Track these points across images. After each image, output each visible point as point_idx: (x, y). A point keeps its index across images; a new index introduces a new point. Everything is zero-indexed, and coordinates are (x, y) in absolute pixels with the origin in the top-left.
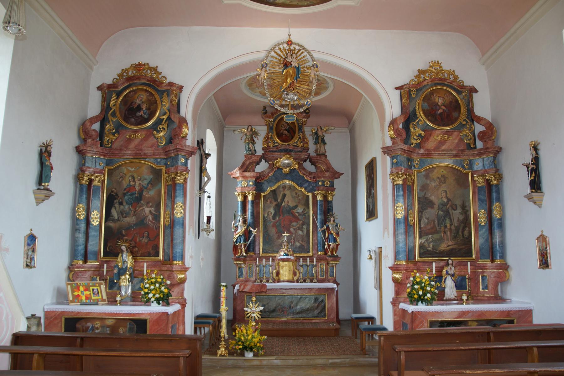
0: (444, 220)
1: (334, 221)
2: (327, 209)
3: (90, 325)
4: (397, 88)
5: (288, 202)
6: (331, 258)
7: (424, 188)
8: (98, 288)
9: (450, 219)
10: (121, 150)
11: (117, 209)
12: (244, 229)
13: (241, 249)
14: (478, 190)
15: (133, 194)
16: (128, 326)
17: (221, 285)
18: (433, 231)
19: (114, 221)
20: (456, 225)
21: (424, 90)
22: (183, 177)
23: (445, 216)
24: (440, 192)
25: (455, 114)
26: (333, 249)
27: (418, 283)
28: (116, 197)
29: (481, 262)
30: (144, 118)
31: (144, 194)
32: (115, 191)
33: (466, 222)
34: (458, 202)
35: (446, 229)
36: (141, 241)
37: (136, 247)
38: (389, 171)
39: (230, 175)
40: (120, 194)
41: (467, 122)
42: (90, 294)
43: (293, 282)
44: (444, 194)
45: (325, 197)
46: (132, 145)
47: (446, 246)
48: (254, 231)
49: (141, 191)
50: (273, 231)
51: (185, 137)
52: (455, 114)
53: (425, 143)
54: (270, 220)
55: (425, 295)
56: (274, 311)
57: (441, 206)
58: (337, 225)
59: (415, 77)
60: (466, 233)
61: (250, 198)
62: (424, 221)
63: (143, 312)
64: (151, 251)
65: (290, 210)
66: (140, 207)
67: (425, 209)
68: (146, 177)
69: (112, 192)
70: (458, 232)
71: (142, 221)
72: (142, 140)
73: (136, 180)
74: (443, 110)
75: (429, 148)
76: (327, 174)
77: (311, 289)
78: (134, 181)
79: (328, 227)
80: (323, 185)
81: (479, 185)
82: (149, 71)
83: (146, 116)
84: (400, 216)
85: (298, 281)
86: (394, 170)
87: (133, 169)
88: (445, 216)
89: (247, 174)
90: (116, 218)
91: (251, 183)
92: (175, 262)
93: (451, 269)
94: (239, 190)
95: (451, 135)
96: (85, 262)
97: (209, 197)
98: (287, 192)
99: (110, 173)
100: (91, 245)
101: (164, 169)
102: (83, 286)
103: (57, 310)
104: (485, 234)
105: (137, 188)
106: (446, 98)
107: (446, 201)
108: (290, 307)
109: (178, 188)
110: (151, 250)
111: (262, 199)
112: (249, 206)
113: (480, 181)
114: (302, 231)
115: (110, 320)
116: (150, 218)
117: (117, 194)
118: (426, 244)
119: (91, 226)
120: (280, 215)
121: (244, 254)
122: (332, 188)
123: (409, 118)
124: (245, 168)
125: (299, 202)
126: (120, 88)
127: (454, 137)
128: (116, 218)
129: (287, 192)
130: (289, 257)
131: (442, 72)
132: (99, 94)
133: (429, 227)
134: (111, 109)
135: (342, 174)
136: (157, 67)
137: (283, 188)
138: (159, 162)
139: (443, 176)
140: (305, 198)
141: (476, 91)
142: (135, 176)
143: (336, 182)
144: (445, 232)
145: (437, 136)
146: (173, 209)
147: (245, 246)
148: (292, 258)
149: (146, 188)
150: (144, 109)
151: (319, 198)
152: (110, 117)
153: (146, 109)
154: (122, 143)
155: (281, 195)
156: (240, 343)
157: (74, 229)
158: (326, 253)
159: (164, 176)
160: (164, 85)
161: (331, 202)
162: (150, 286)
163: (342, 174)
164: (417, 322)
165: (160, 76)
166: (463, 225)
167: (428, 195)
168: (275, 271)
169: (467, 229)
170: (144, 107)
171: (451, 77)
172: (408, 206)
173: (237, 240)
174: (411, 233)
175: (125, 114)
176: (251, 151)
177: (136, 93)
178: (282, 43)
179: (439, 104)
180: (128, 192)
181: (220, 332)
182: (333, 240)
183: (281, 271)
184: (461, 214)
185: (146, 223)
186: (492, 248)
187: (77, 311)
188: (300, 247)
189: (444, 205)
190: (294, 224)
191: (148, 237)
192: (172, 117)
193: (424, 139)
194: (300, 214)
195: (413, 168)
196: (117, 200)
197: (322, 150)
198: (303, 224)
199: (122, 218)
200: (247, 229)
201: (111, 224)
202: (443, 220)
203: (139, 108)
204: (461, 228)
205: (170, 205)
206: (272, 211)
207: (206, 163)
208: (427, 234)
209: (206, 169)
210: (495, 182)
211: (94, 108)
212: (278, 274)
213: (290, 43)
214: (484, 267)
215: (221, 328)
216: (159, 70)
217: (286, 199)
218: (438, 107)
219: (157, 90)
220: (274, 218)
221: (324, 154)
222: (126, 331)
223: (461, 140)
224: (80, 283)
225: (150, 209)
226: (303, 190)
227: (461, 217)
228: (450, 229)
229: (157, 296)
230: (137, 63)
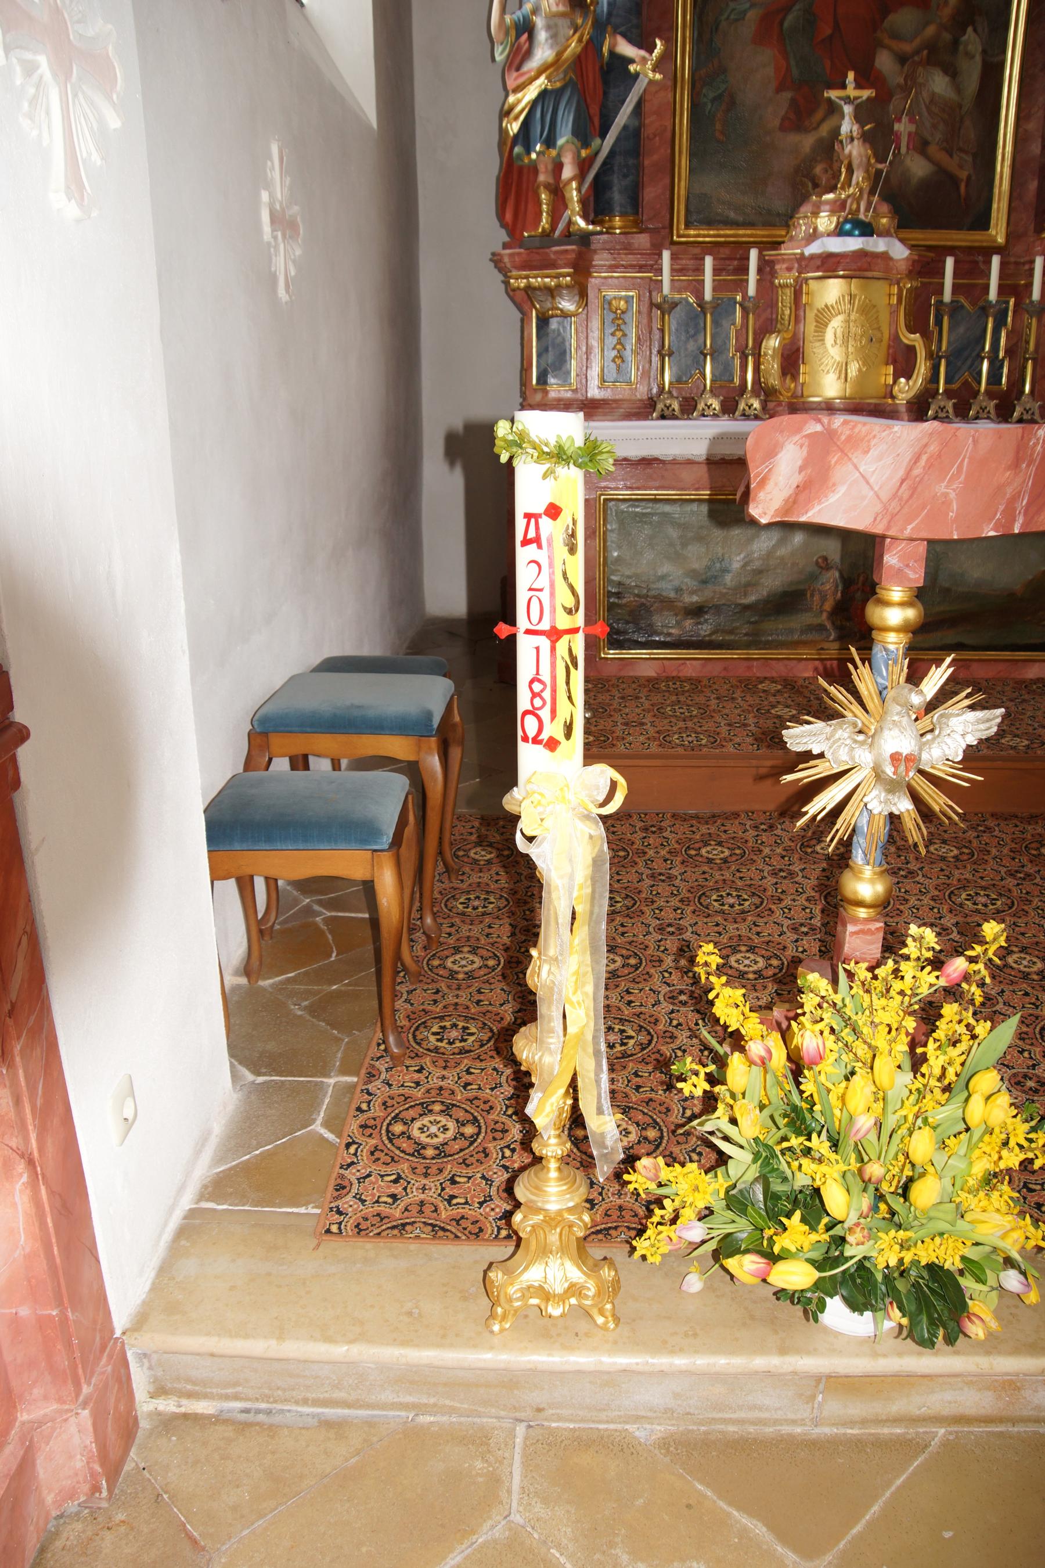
48: (644, 64)
121: (582, 223)
130: (878, 245)
148: (899, 251)
168: (773, 343)
173: (526, 125)
188: (925, 185)
200: (592, 46)
212: (792, 359)
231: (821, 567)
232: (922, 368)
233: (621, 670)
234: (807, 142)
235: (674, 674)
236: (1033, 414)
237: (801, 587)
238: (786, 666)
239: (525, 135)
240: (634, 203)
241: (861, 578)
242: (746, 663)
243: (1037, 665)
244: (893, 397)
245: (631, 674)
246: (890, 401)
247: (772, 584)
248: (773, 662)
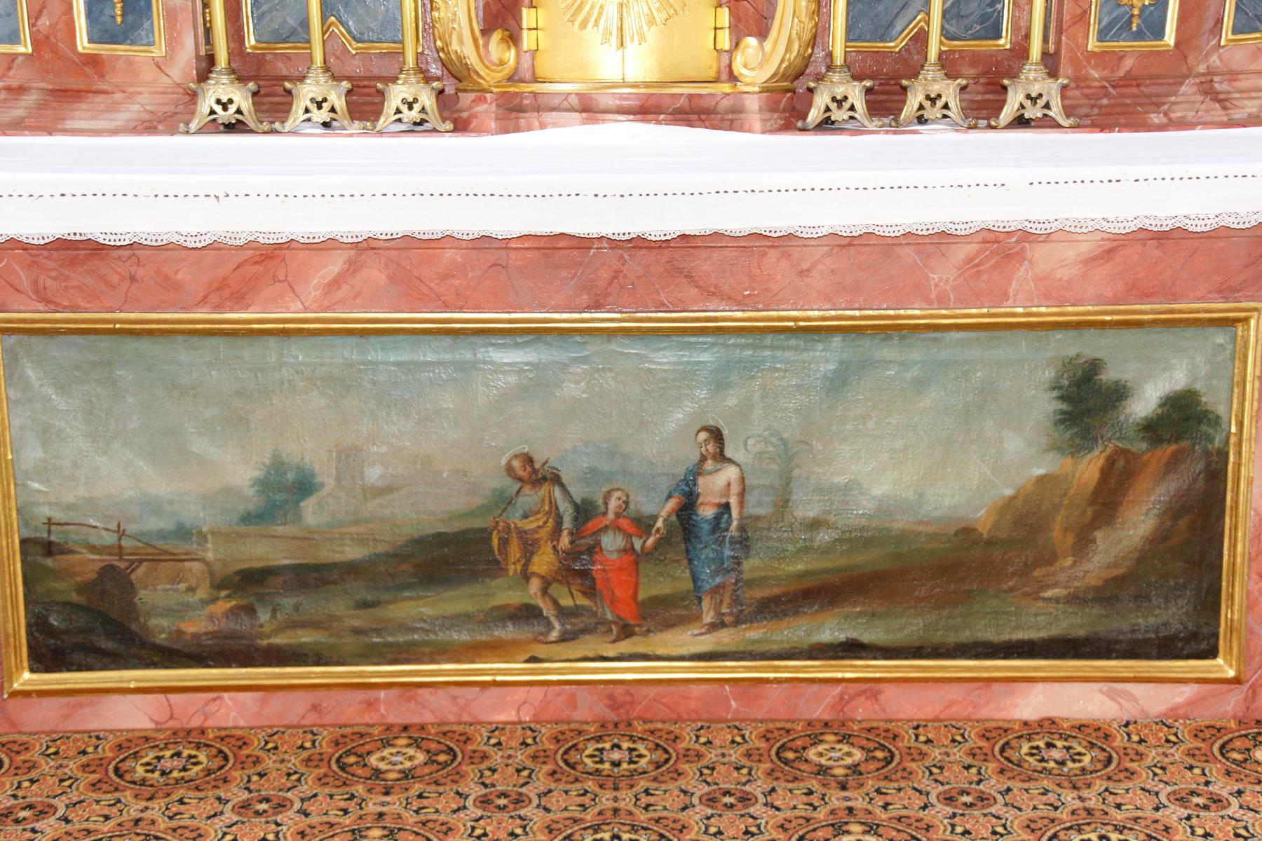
56: (450, 557)
77: (1003, 248)
85: (790, 105)
108: (688, 506)
231: (520, 479)
233: (67, 717)
235: (196, 723)
236: (1047, 106)
237: (477, 523)
238: (455, 698)
241: (613, 503)
242: (361, 695)
243: (1040, 686)
244: (733, 78)
245: (93, 725)
246: (726, 88)
247: (433, 508)
248: (425, 692)
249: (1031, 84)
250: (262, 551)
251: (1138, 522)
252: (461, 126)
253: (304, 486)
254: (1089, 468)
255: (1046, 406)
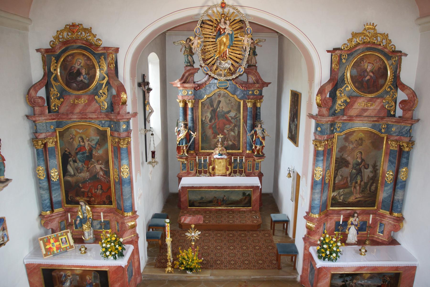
0: (356, 177)
1: (261, 127)
2: (256, 116)
3: (63, 273)
4: (328, 51)
5: (222, 108)
6: (258, 158)
7: (342, 149)
8: (66, 236)
9: (361, 176)
10: (67, 115)
11: (72, 165)
12: (185, 133)
13: (183, 149)
14: (390, 152)
15: (83, 154)
16: (93, 275)
17: (166, 222)
18: (345, 186)
19: (71, 176)
20: (366, 181)
21: (355, 54)
22: (126, 142)
23: (357, 174)
24: (355, 153)
25: (381, 81)
26: (259, 150)
27: (326, 243)
28: (70, 156)
29: (381, 211)
30: (84, 82)
31: (94, 153)
32: (68, 151)
33: (374, 179)
34: (371, 163)
35: (357, 185)
36: (96, 192)
37: (92, 197)
38: (312, 138)
39: (172, 84)
40: (73, 153)
41: (391, 89)
42: (60, 244)
43: (226, 176)
44: (359, 155)
45: (254, 105)
46: (77, 110)
47: (354, 198)
48: (194, 135)
49: (91, 150)
50: (209, 132)
51: (124, 103)
52: (381, 81)
53: (349, 110)
54: (207, 123)
55: (331, 254)
57: (355, 166)
58: (263, 130)
59: (348, 41)
60: (373, 188)
61: (190, 105)
62: (339, 178)
63: (103, 265)
64: (106, 201)
65: (224, 115)
66: (91, 164)
67: (341, 168)
68: (94, 138)
69: (66, 151)
70: (366, 187)
71: (95, 176)
72: (85, 105)
73: (85, 140)
74: (371, 76)
75: (352, 115)
76: (257, 85)
78: (83, 142)
79: (256, 132)
80: (253, 94)
81: (391, 148)
82: (83, 33)
83: (86, 81)
84: (318, 178)
85: (230, 175)
86: (317, 137)
87: (81, 131)
88: (357, 174)
89: (186, 85)
90: (73, 173)
91: (190, 93)
92: (126, 214)
93: (355, 220)
94: (180, 98)
95: (375, 102)
96: (52, 211)
97: (152, 134)
98: (222, 99)
99: (62, 134)
100: (55, 197)
101: (109, 130)
102: (52, 238)
103: (35, 263)
104: (389, 191)
105: (87, 148)
106: (375, 64)
107: (360, 161)
108: (223, 199)
109: (122, 152)
110: (105, 200)
111: (200, 105)
112: (189, 113)
113: (394, 146)
114: (234, 132)
115: (78, 271)
116: (101, 173)
117: (70, 154)
118: (338, 197)
119: (52, 182)
120: (216, 119)
121: (186, 154)
122: (260, 97)
123: (336, 82)
124: (185, 80)
125: (232, 108)
126: (58, 52)
127: (377, 103)
128: (73, 173)
129: (222, 99)
130: (223, 157)
131: (376, 35)
132: (39, 55)
133: (342, 183)
134: (53, 74)
135: (270, 83)
136: (91, 28)
137: (218, 95)
138: (104, 124)
139: (361, 139)
140: (237, 104)
141: (406, 55)
142: (84, 137)
143: (265, 90)
144: (355, 187)
145: (360, 104)
146: (120, 171)
147: (186, 147)
149: (95, 148)
150: (84, 74)
151: (249, 105)
152: (53, 82)
153: (86, 74)
154: (67, 108)
155: (217, 101)
156: (183, 266)
157: (39, 187)
158: (253, 152)
159: (109, 139)
160: (100, 49)
161: (260, 108)
162: (107, 245)
163: (270, 83)
164: (322, 274)
165: (95, 39)
166: (371, 181)
167: (345, 156)
169: (375, 184)
170: (83, 71)
171: (384, 41)
172: (326, 167)
173: (179, 143)
174: (326, 189)
175: (66, 79)
176: (189, 62)
177: (73, 58)
178: (215, 6)
179: (368, 70)
180: (80, 151)
181: (167, 256)
182: (259, 143)
183: (216, 167)
184: (371, 172)
185: (98, 178)
186: (393, 202)
187: (50, 264)
188: (231, 145)
189: (358, 164)
190: (227, 126)
191: (101, 189)
192: (111, 82)
193: (348, 105)
194: (232, 118)
195: (335, 131)
196: (71, 159)
197: (253, 62)
198: (235, 126)
199: (77, 174)
201: (69, 179)
202: (355, 177)
203: (79, 73)
204: (369, 184)
205: (117, 164)
206: (209, 115)
207: (149, 97)
208: (340, 189)
209: (149, 103)
210: (407, 149)
211: (37, 73)
212: (213, 169)
213: (223, 5)
214: (383, 216)
215: (167, 252)
216: (93, 32)
217: (221, 105)
218: (366, 74)
219: (93, 54)
220: (210, 121)
221: (255, 66)
222: (92, 278)
223: (383, 107)
224: (50, 236)
225: (101, 166)
226: (235, 97)
227: (371, 175)
228: (360, 184)
229: (113, 253)
230: (71, 24)
232: (230, 170)
234: (216, 140)
239: (179, 144)
240: (194, 149)
247: (209, 199)
249: (243, 174)
250: (201, 201)
251: (247, 200)
252: (211, 176)
253: (203, 198)
254: (244, 197)
255: (242, 194)
